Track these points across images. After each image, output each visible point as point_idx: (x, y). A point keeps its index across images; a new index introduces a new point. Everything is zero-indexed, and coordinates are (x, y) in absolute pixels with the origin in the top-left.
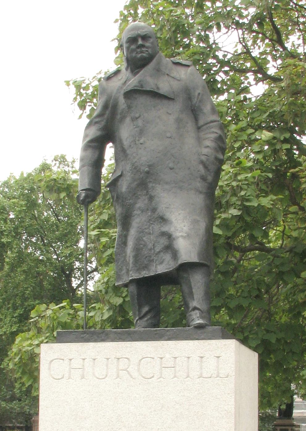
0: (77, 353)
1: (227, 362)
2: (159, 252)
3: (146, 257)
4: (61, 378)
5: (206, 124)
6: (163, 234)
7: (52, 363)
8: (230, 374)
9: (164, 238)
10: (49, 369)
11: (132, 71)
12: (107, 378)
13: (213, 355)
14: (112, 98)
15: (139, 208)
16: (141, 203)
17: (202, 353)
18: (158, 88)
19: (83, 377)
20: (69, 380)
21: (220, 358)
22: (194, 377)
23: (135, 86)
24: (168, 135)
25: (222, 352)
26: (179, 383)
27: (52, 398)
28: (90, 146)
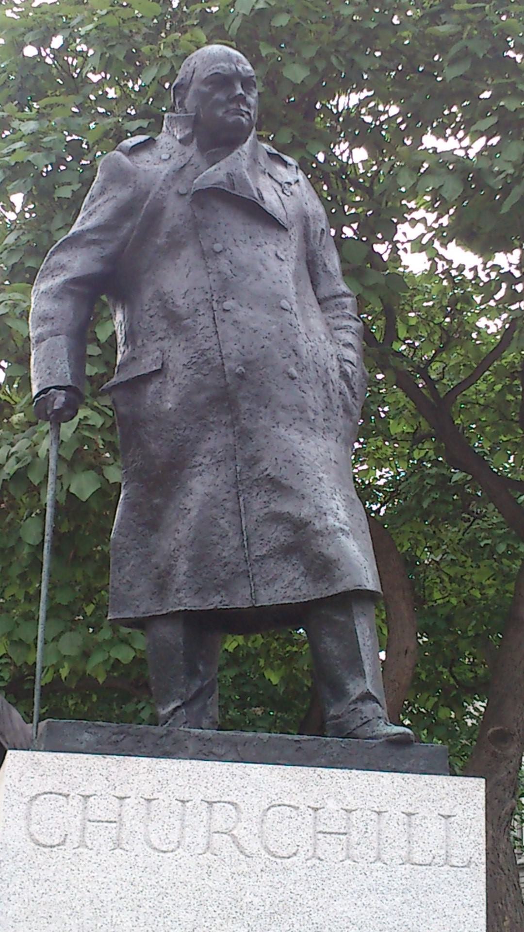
0: (106, 782)
1: (467, 831)
2: (263, 557)
3: (226, 565)
4: (58, 845)
5: (335, 297)
6: (277, 518)
7: (37, 802)
8: (473, 860)
9: (280, 527)
10: (28, 817)
11: (202, 149)
12: (180, 850)
13: (436, 813)
14: (151, 196)
15: (212, 452)
16: (216, 441)
17: (411, 805)
18: (262, 199)
19: (118, 844)
20: (81, 850)
21: (453, 819)
22: (392, 860)
23: (221, 183)
24: (285, 303)
25: (455, 806)
26: (357, 873)
27: (32, 896)
28: (72, 292)
